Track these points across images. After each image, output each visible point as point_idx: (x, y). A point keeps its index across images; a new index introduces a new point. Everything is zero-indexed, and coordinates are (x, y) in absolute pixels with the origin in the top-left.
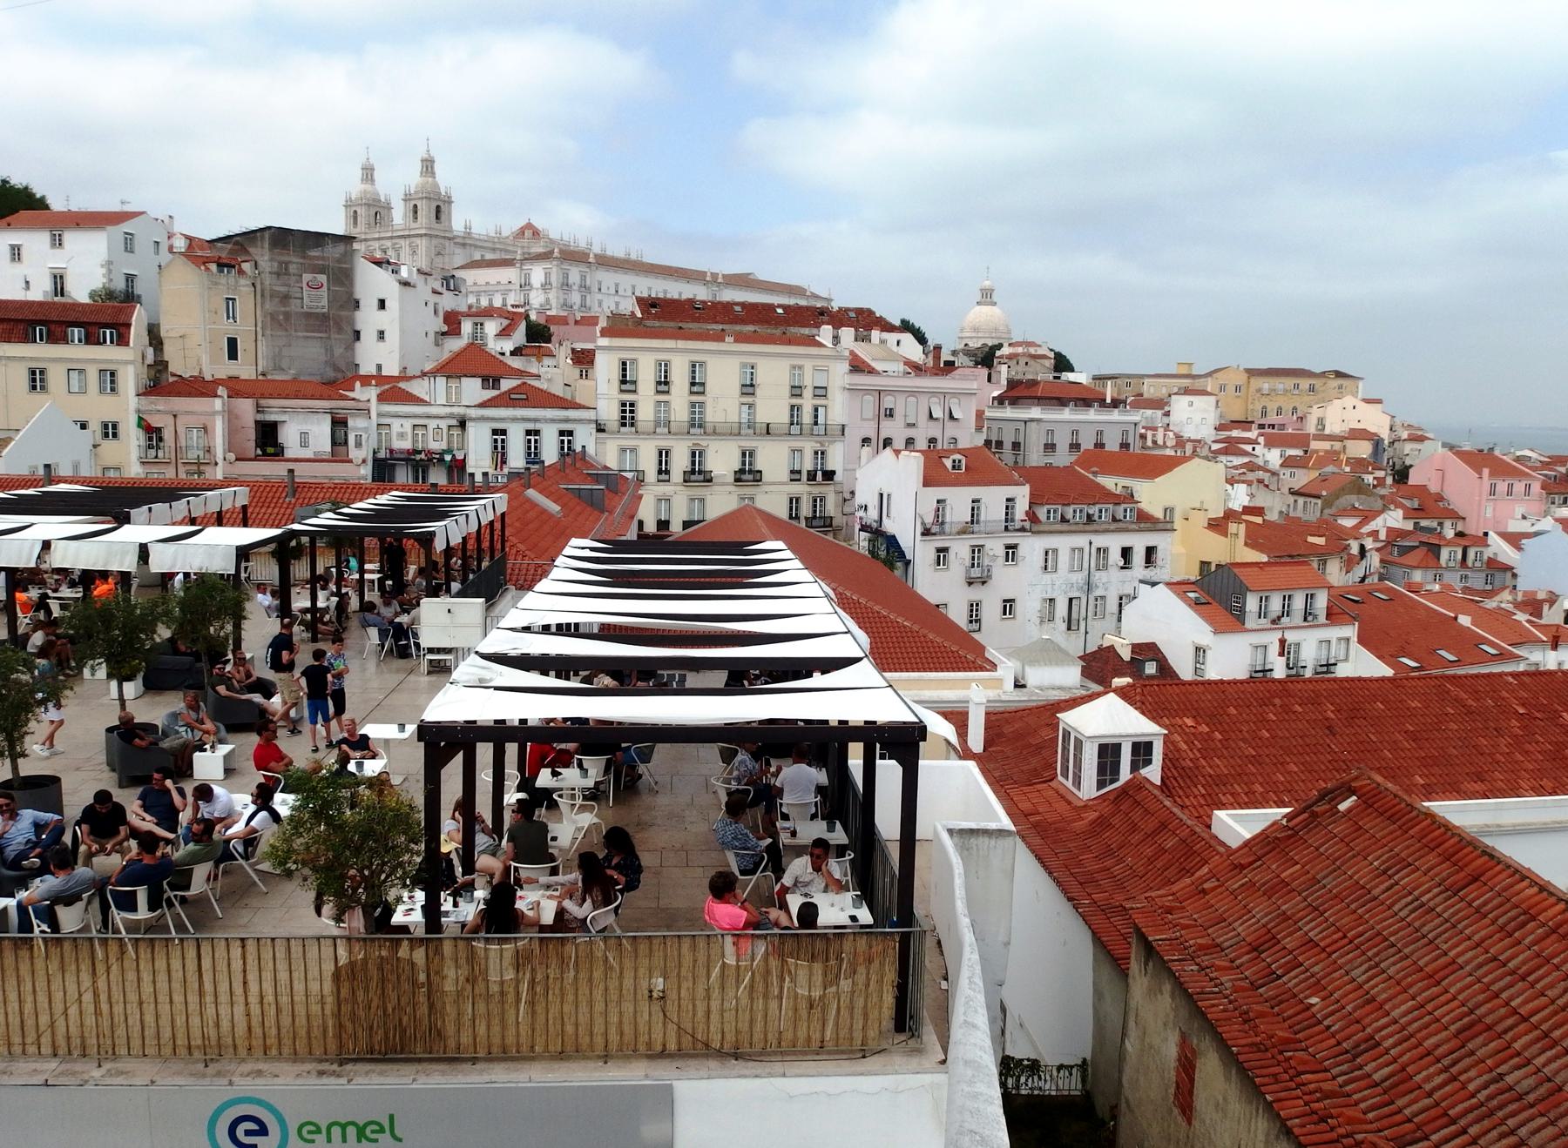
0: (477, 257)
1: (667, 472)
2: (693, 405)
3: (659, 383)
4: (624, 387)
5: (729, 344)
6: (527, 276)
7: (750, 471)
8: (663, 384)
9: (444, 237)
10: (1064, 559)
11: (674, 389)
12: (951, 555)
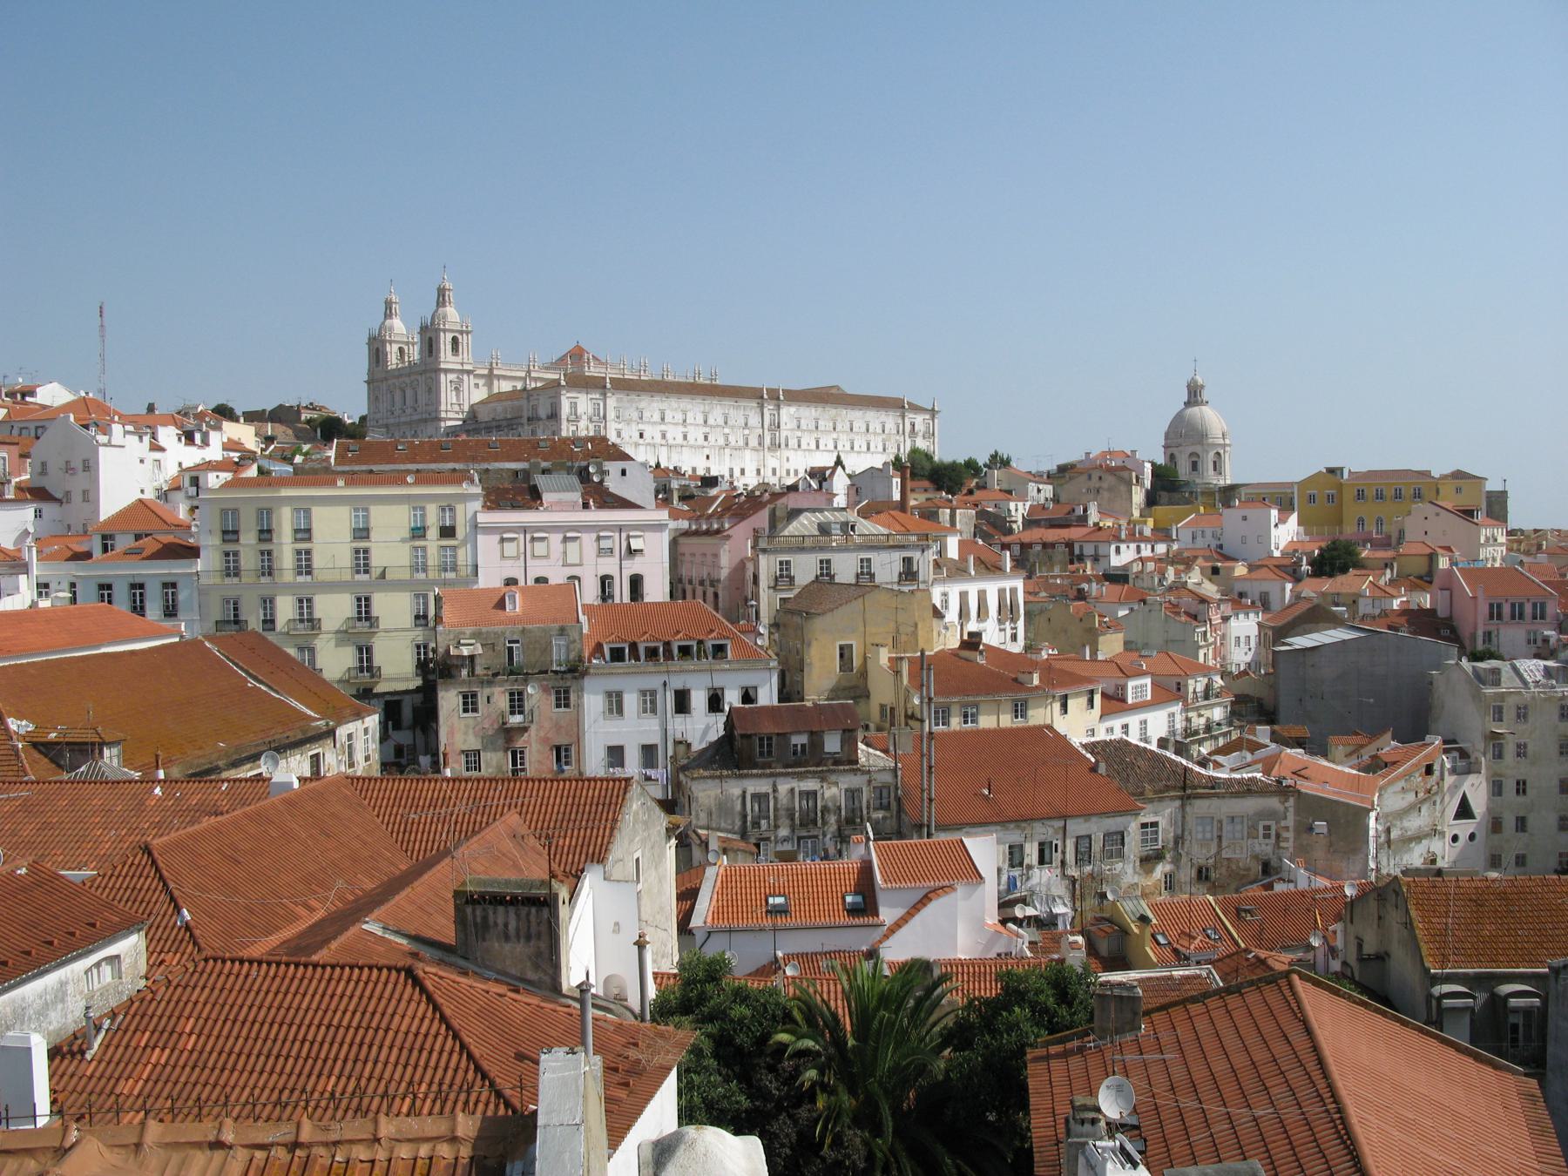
0: (506, 386)
1: (272, 621)
2: (299, 552)
3: (261, 531)
4: (227, 537)
5: (341, 489)
6: (535, 408)
7: (367, 619)
8: (266, 534)
9: (463, 371)
10: (631, 701)
11: (274, 536)
12: (481, 700)
